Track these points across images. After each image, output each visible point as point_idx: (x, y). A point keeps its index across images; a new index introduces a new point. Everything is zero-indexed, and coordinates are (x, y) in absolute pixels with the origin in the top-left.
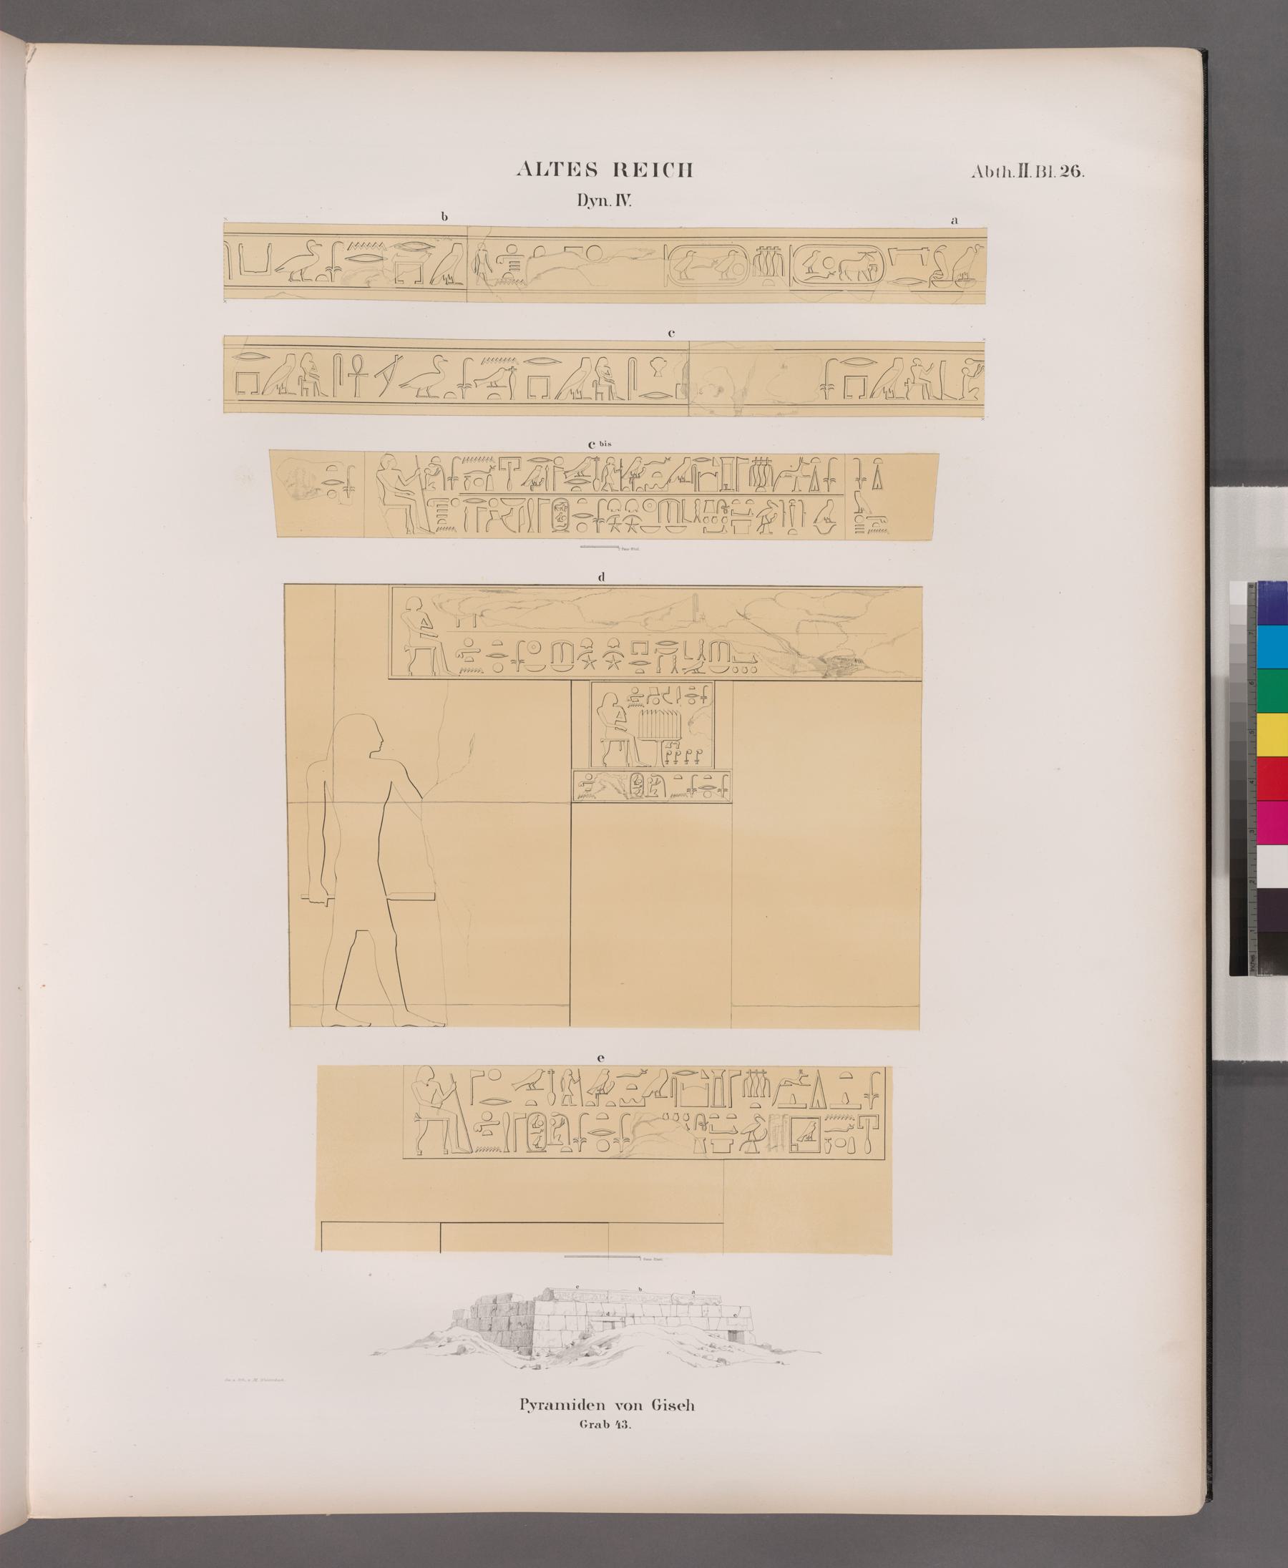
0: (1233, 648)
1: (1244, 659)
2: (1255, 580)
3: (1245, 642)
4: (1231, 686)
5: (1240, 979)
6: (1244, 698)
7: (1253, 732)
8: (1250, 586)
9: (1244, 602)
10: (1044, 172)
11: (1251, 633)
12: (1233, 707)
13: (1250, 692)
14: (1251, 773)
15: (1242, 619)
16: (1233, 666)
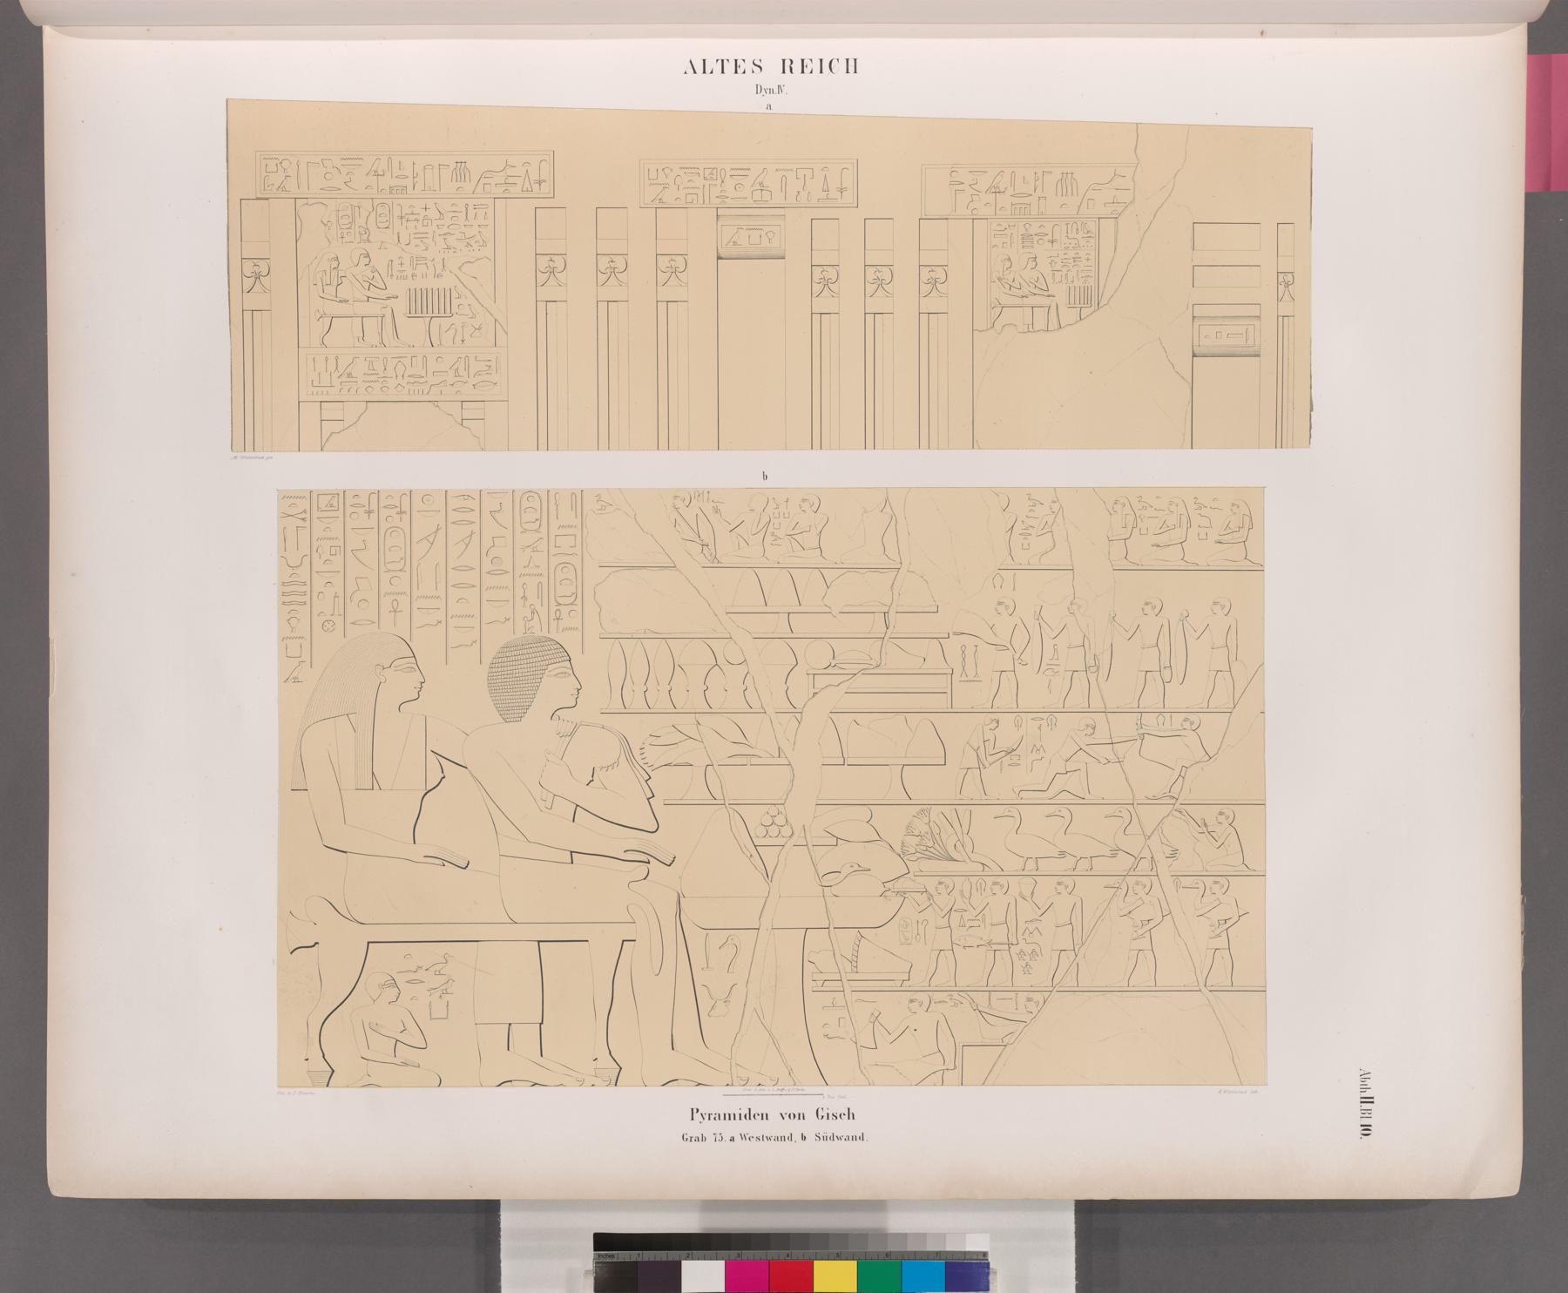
0: (923, 1236)
1: (912, 1247)
2: (990, 1259)
3: (929, 1249)
4: (883, 1236)
5: (590, 1243)
6: (871, 1249)
7: (838, 1257)
8: (985, 1254)
9: (968, 1249)
10: (1366, 1113)
11: (938, 1255)
12: (863, 1236)
13: (878, 1254)
14: (798, 1254)
15: (951, 1246)
16: (904, 1236)
